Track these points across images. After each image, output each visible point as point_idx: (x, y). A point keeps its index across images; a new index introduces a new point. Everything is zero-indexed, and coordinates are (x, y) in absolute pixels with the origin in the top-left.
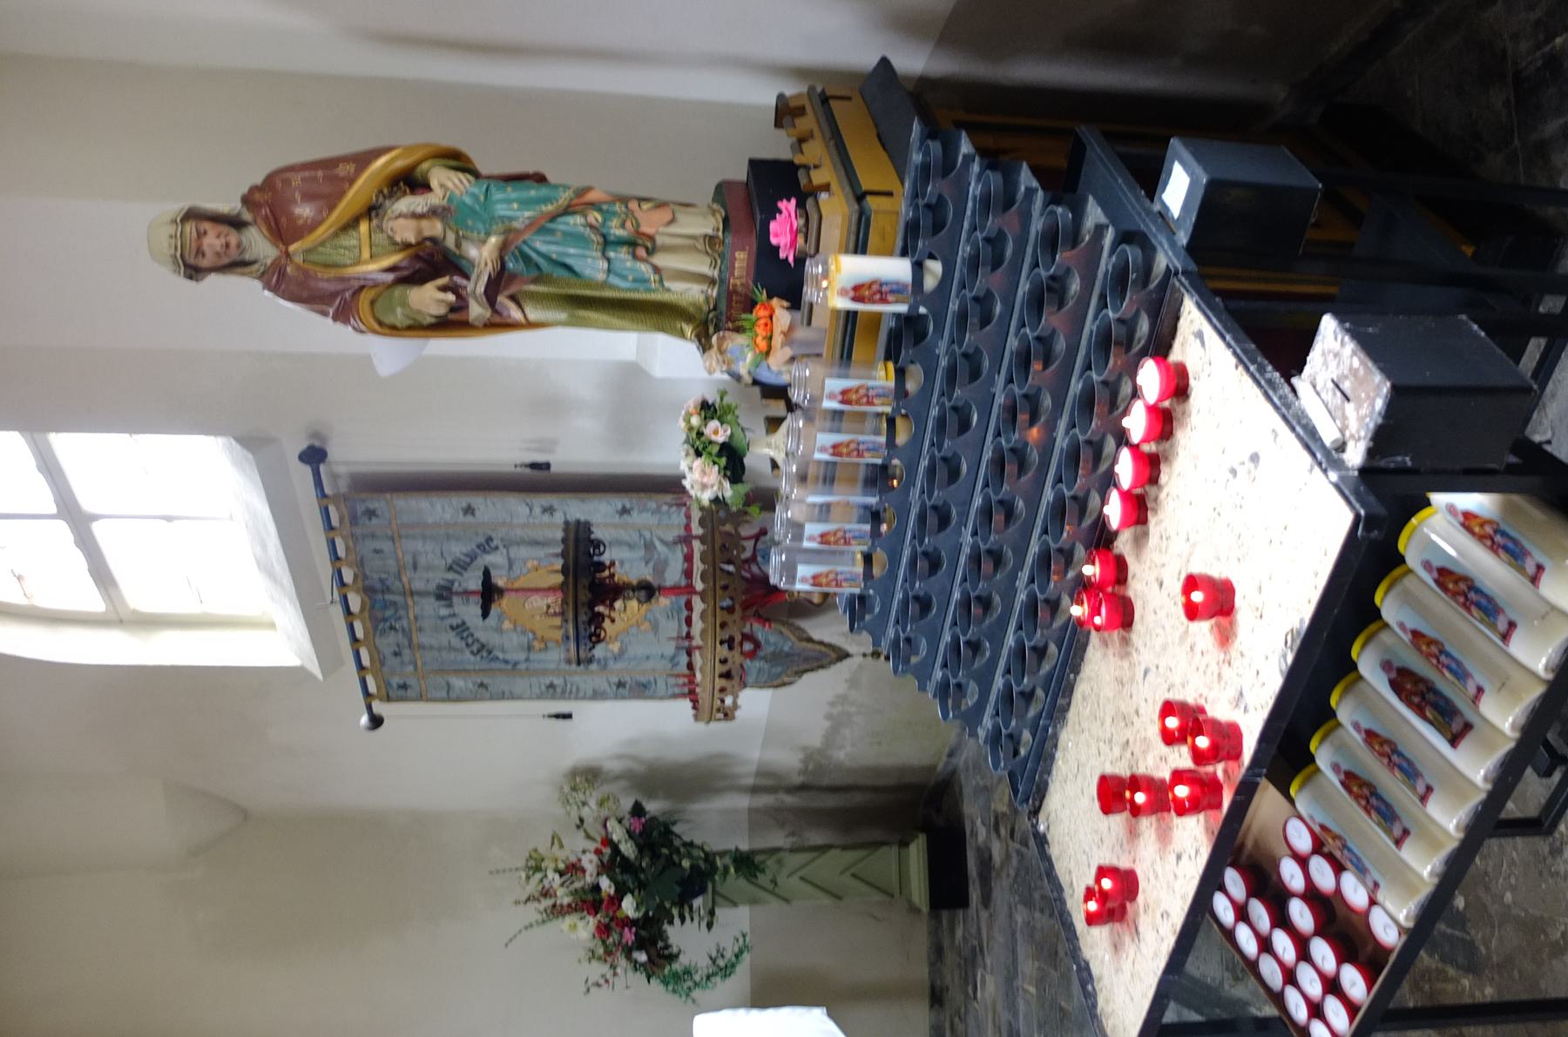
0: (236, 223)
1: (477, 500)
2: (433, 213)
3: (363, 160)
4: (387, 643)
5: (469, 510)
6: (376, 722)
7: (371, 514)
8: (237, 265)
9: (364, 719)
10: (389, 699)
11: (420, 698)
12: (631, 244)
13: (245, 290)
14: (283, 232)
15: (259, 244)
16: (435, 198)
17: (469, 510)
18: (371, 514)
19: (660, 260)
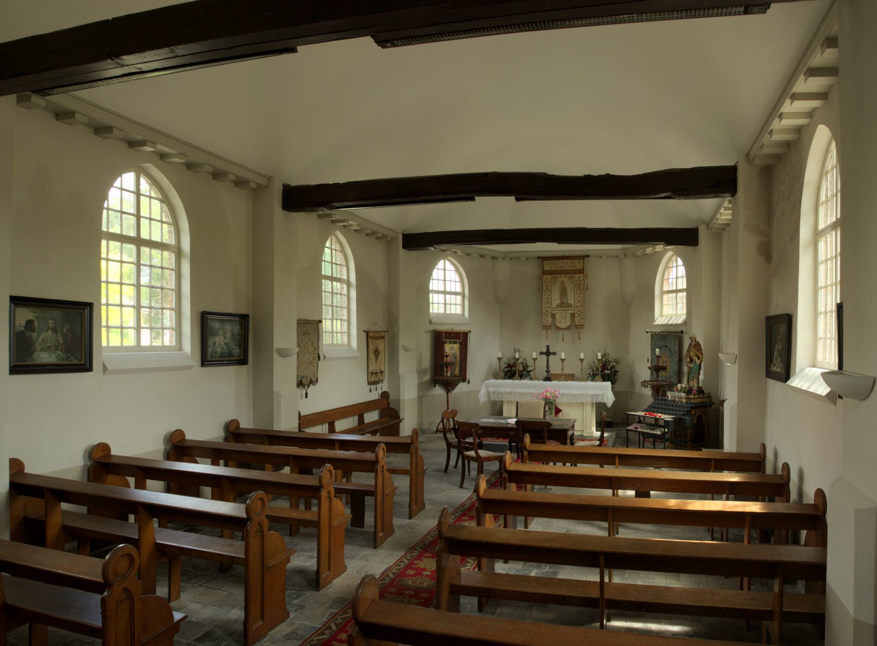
0: (695, 341)
1: (677, 353)
2: (695, 361)
3: (702, 354)
4: (659, 336)
5: (676, 352)
6: (647, 332)
7: (676, 338)
8: (691, 341)
9: (648, 330)
10: (651, 335)
11: (651, 340)
12: (693, 379)
13: (690, 341)
14: (695, 346)
15: (693, 343)
16: (697, 361)
17: (676, 352)
18: (676, 338)
19: (692, 382)
